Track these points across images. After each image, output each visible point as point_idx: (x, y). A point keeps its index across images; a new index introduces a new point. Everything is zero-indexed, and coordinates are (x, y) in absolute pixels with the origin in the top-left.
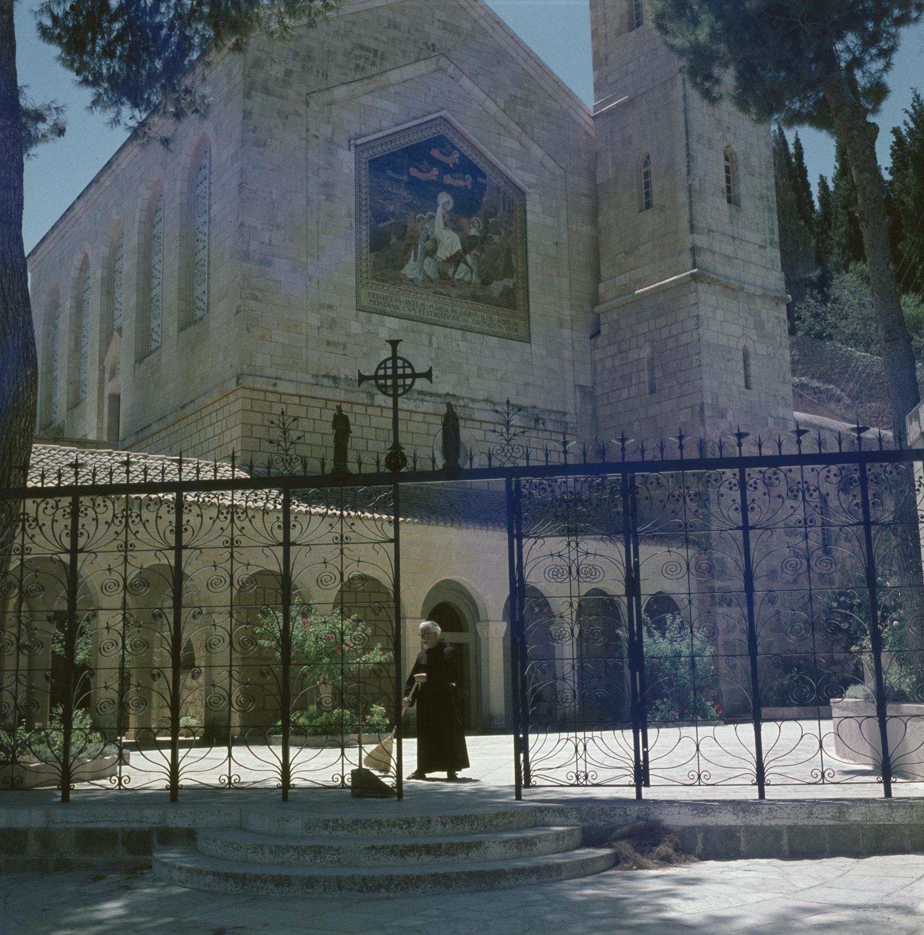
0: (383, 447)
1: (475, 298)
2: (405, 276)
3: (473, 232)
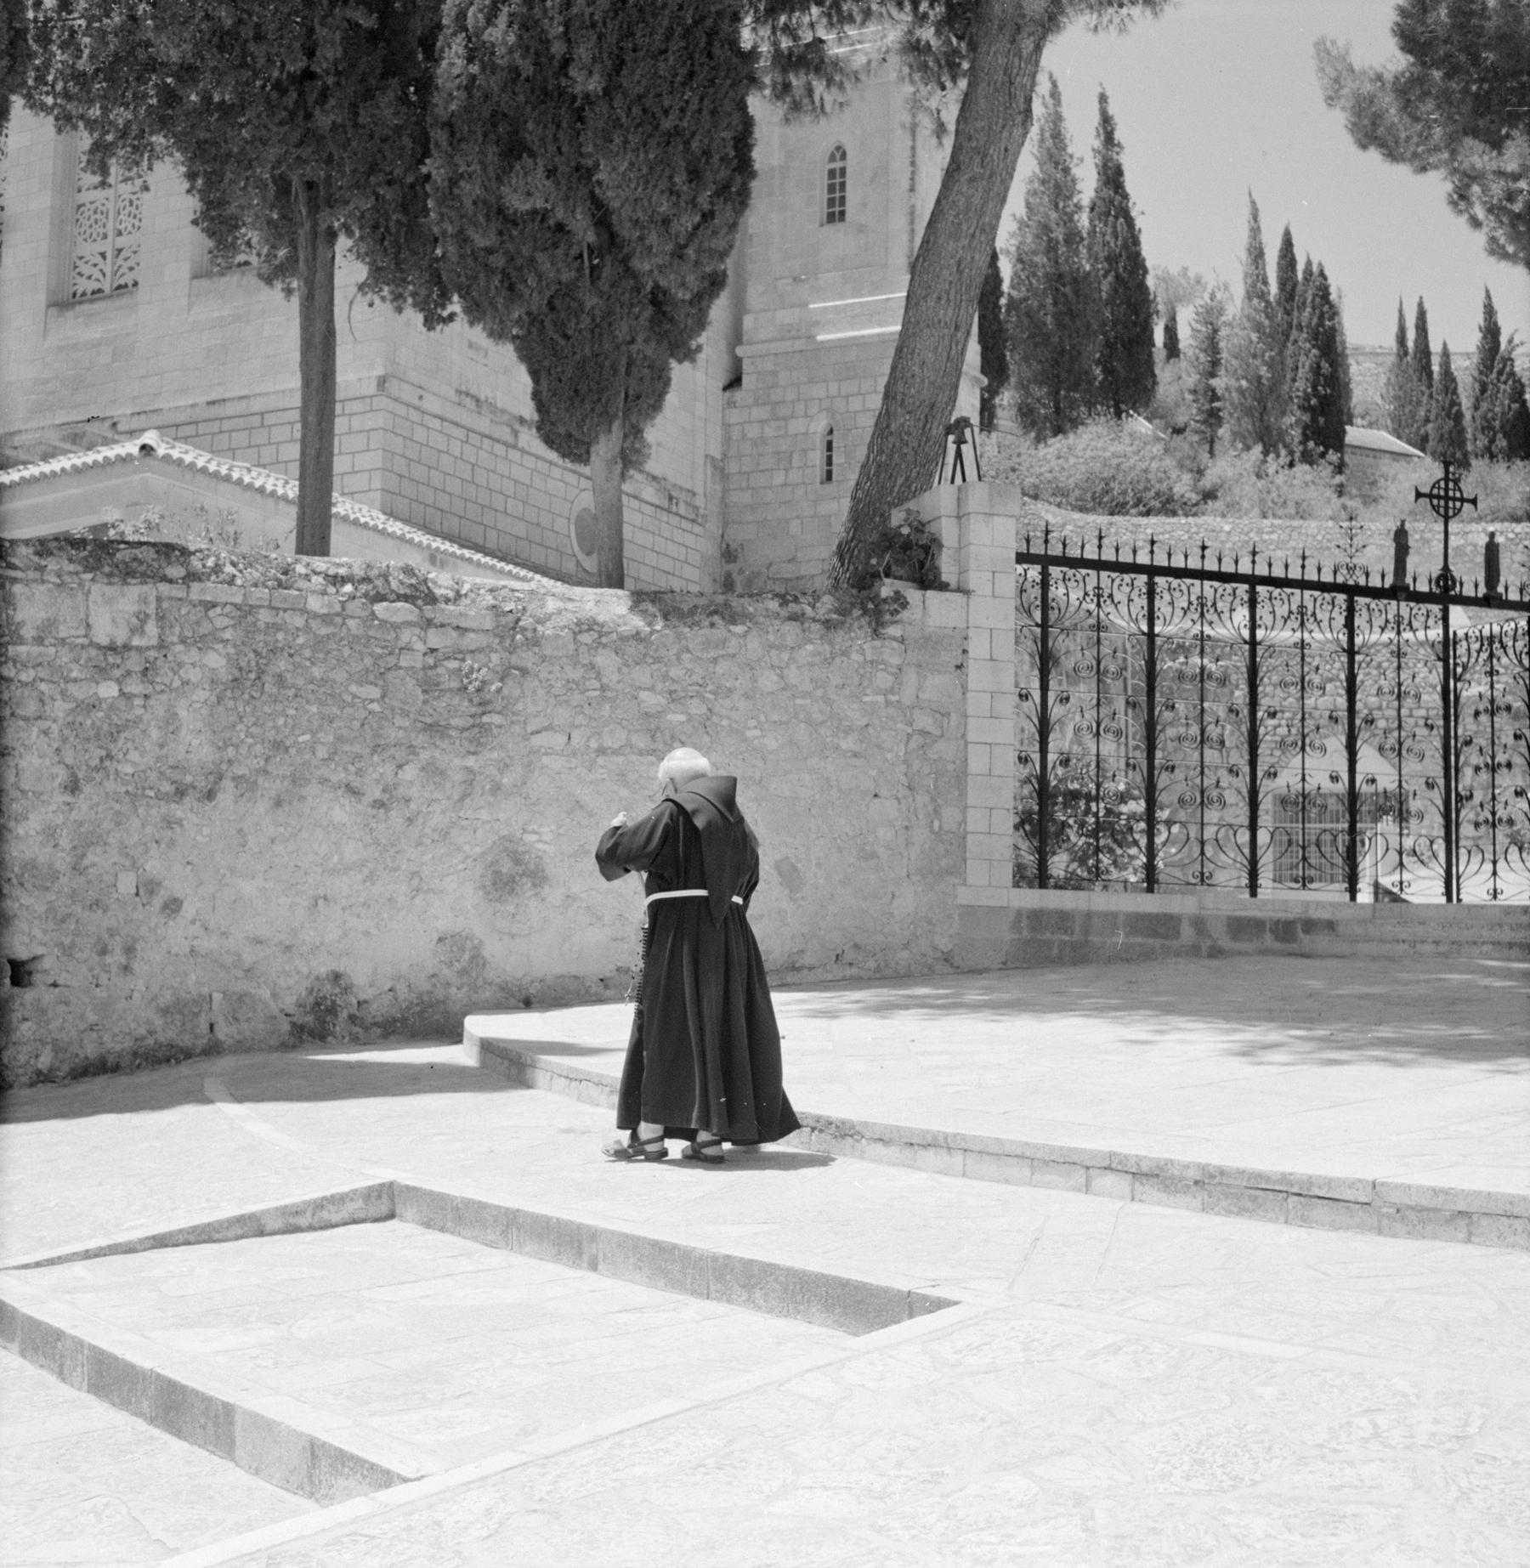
0: (1436, 569)
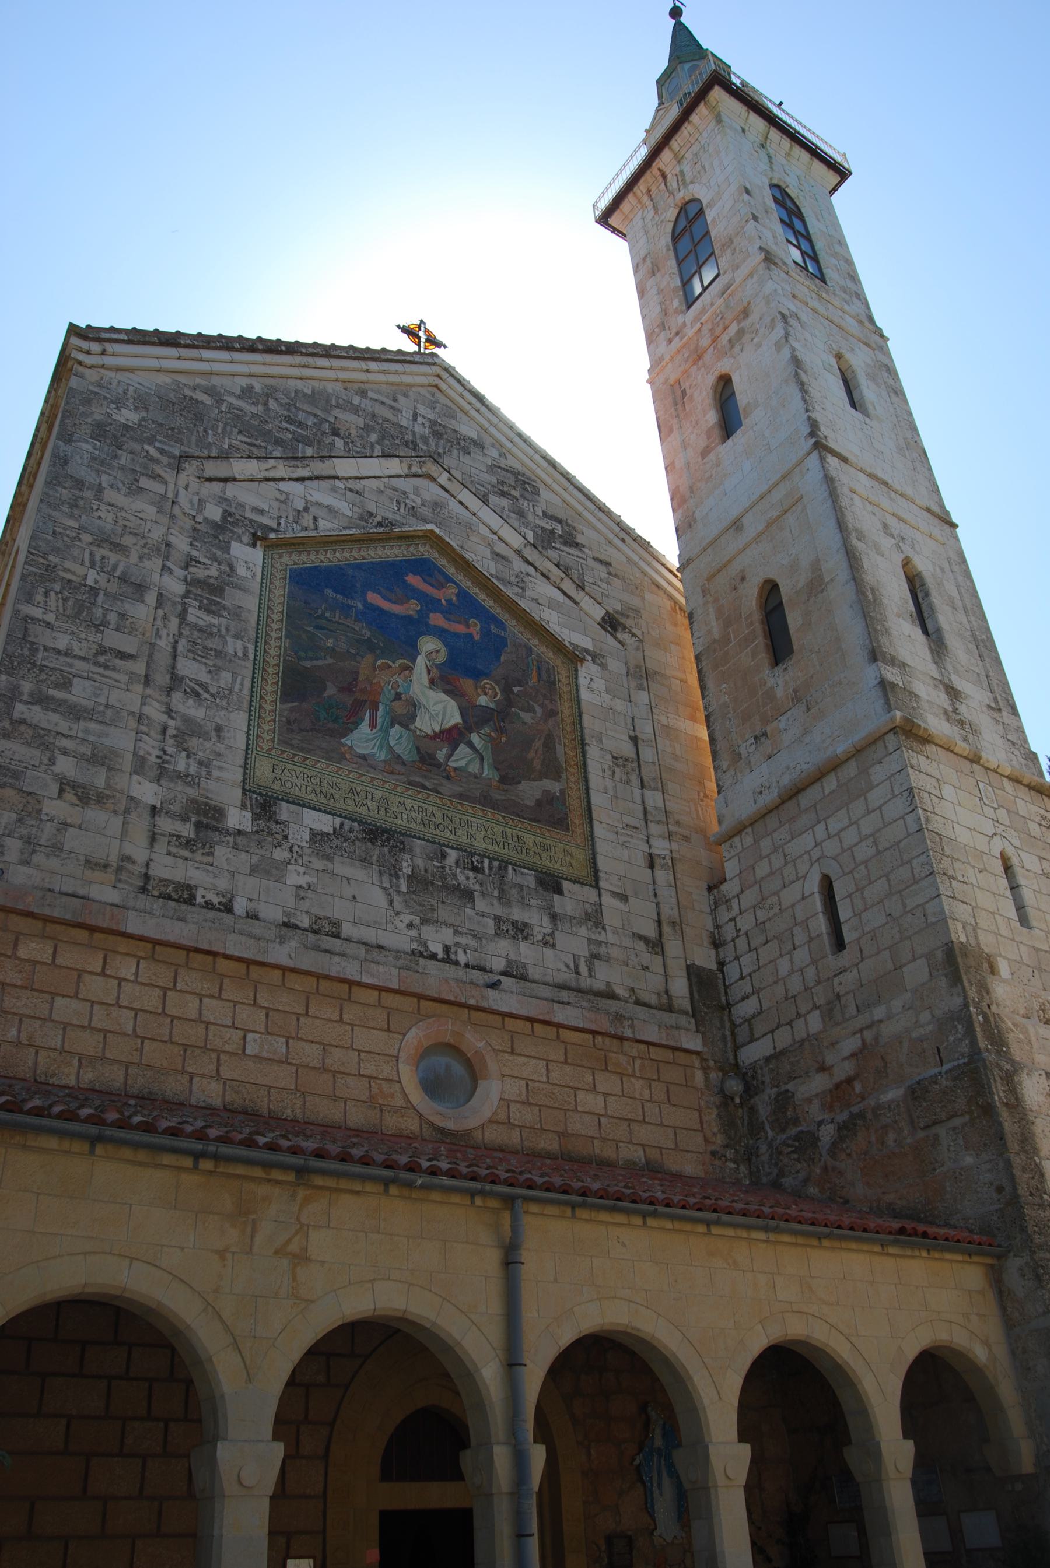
1: (486, 801)
2: (351, 748)
3: (483, 700)
